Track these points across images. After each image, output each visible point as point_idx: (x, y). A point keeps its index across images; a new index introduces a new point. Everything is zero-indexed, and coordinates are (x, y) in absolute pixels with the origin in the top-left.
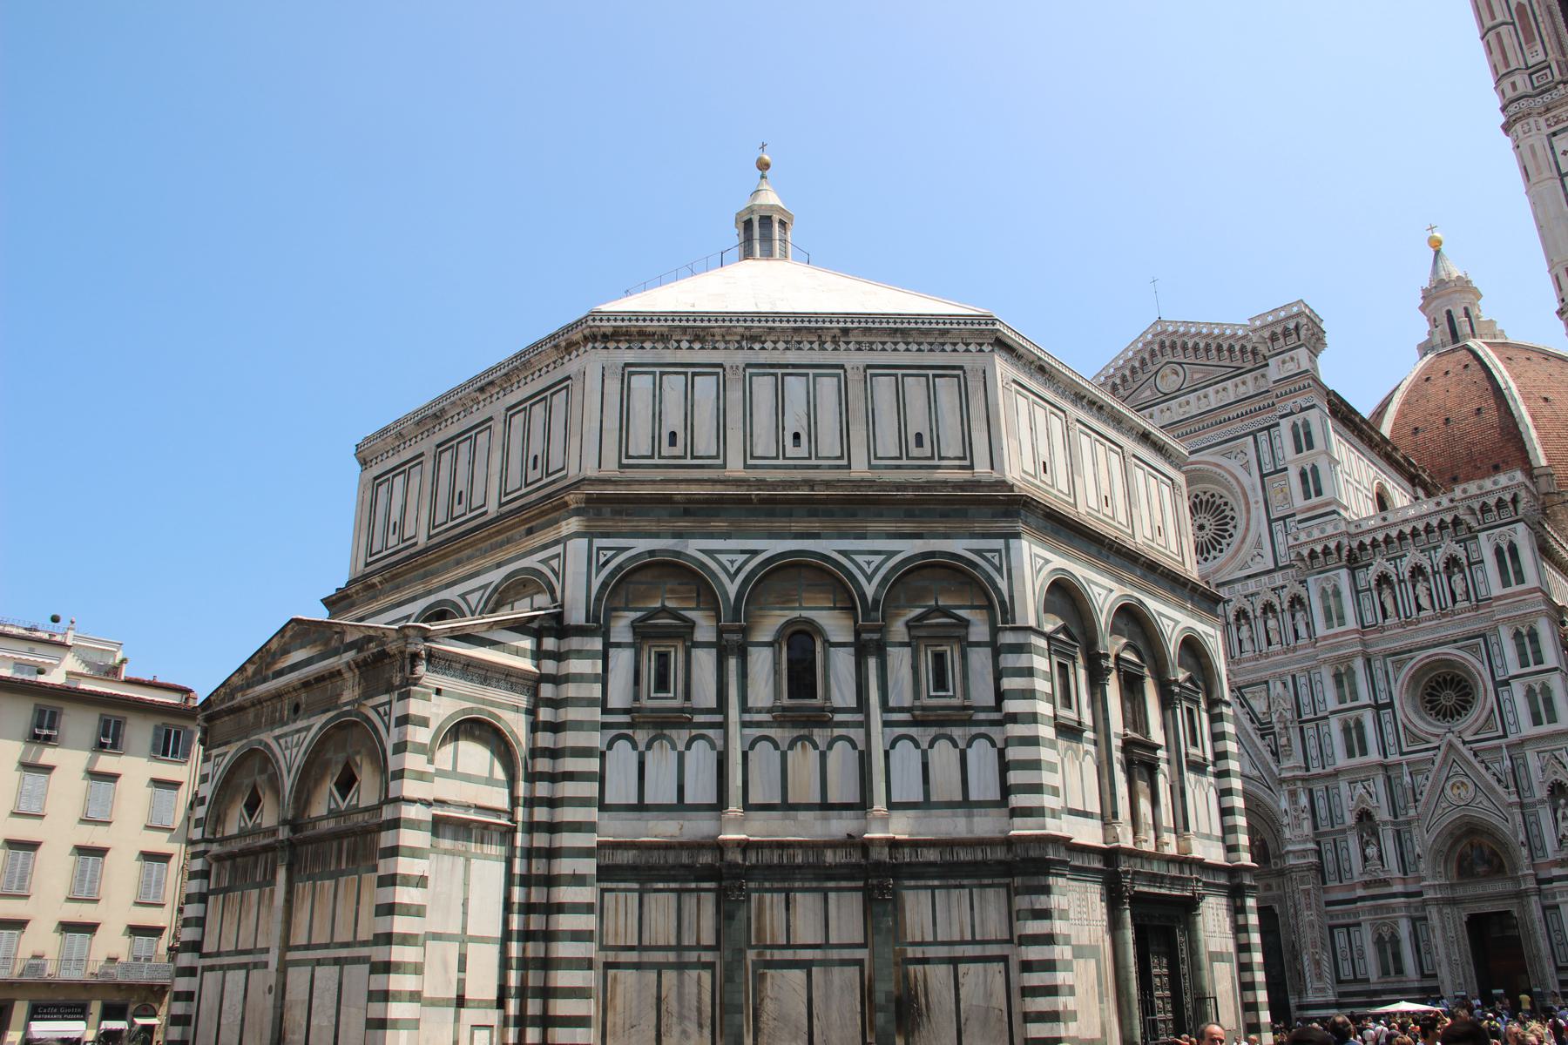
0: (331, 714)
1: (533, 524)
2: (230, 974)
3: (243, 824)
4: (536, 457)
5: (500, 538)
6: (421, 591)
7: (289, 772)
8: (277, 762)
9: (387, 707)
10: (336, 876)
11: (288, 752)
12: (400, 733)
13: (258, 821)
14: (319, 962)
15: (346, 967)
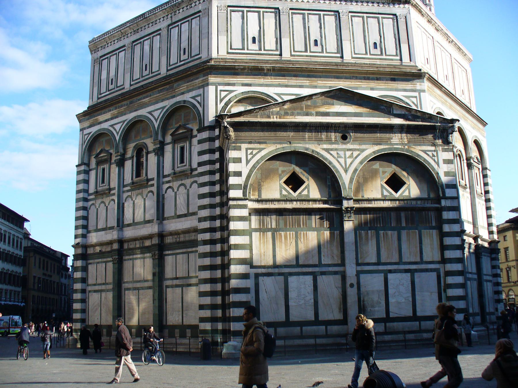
0: (382, 147)
1: (396, 77)
2: (292, 280)
3: (284, 192)
4: (375, 44)
5: (371, 76)
6: (308, 84)
7: (346, 171)
8: (330, 163)
9: (435, 153)
10: (399, 229)
11: (342, 161)
12: (448, 167)
13: (305, 192)
14: (390, 271)
15: (416, 275)
